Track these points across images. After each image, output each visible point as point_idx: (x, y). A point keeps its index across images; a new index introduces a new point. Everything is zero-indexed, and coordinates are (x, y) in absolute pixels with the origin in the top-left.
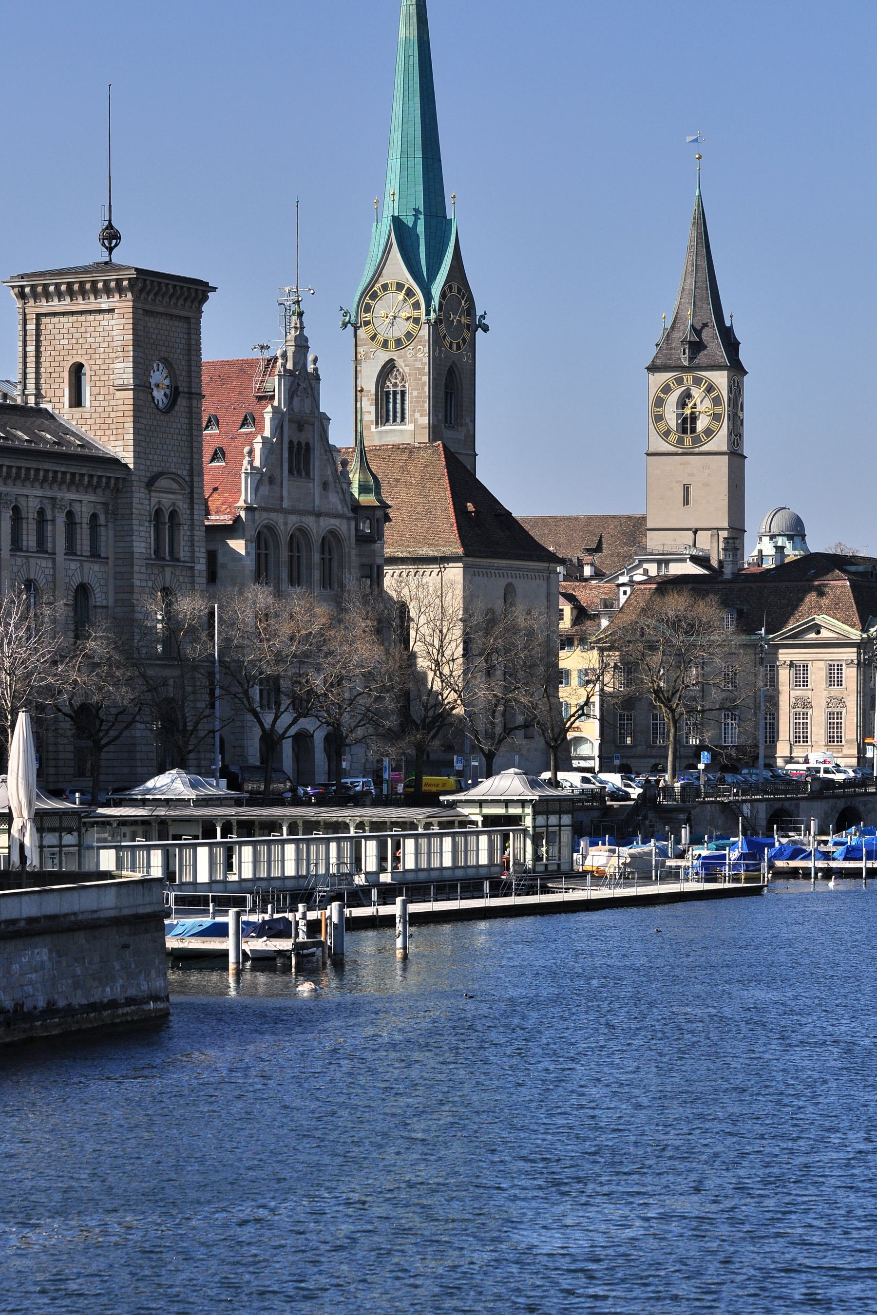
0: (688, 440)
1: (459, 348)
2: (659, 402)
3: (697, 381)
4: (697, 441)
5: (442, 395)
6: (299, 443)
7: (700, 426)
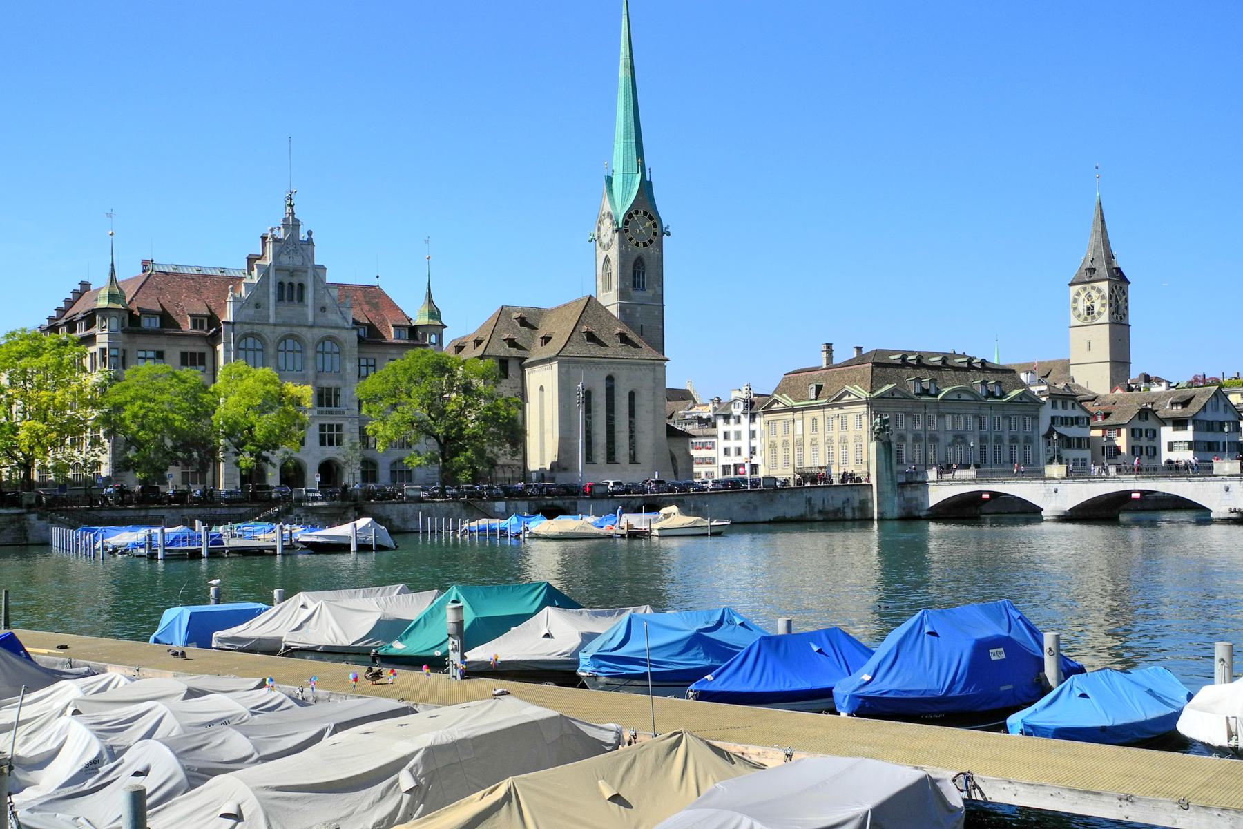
0: (1089, 317)
1: (645, 245)
2: (1075, 301)
3: (1093, 288)
4: (1093, 318)
5: (630, 272)
6: (291, 284)
7: (1096, 310)
